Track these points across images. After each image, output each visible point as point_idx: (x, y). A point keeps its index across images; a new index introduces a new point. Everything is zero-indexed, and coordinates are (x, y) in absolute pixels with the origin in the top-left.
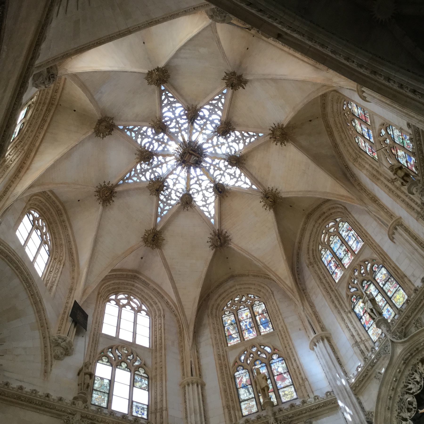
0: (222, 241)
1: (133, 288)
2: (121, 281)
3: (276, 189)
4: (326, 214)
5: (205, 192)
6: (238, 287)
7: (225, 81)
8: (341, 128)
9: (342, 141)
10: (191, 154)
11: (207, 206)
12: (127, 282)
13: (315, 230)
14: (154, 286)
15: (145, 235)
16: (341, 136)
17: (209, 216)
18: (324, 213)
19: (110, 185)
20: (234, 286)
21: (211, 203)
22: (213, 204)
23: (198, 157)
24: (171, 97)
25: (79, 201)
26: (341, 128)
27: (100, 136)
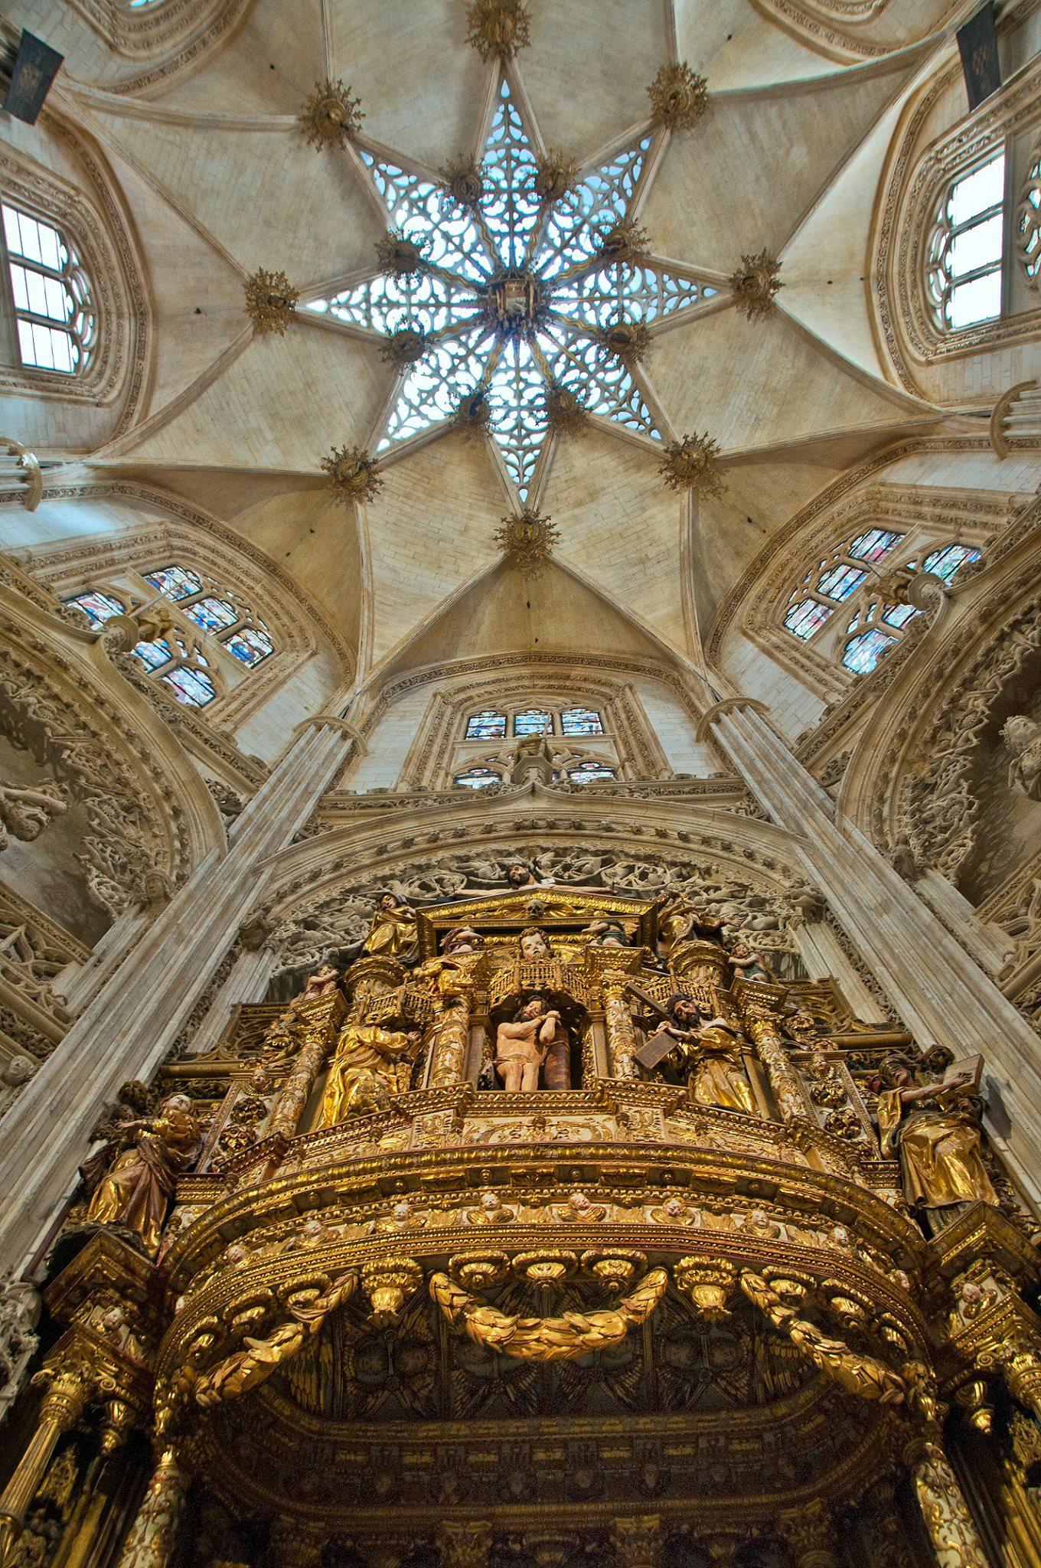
0: (357, 481)
1: (114, 318)
2: (118, 274)
3: (558, 534)
4: (568, 683)
5: (444, 388)
6: (258, 589)
7: (742, 266)
8: (785, 580)
9: (760, 598)
10: (527, 295)
11: (413, 412)
12: (122, 292)
13: (513, 684)
14: (146, 372)
15: (271, 277)
16: (766, 592)
17: (391, 430)
18: (568, 677)
19: (357, 122)
20: (254, 579)
21: (424, 417)
22: (426, 424)
23: (527, 312)
24: (632, 178)
25: (272, 67)
26: (785, 580)
27: (472, 27)
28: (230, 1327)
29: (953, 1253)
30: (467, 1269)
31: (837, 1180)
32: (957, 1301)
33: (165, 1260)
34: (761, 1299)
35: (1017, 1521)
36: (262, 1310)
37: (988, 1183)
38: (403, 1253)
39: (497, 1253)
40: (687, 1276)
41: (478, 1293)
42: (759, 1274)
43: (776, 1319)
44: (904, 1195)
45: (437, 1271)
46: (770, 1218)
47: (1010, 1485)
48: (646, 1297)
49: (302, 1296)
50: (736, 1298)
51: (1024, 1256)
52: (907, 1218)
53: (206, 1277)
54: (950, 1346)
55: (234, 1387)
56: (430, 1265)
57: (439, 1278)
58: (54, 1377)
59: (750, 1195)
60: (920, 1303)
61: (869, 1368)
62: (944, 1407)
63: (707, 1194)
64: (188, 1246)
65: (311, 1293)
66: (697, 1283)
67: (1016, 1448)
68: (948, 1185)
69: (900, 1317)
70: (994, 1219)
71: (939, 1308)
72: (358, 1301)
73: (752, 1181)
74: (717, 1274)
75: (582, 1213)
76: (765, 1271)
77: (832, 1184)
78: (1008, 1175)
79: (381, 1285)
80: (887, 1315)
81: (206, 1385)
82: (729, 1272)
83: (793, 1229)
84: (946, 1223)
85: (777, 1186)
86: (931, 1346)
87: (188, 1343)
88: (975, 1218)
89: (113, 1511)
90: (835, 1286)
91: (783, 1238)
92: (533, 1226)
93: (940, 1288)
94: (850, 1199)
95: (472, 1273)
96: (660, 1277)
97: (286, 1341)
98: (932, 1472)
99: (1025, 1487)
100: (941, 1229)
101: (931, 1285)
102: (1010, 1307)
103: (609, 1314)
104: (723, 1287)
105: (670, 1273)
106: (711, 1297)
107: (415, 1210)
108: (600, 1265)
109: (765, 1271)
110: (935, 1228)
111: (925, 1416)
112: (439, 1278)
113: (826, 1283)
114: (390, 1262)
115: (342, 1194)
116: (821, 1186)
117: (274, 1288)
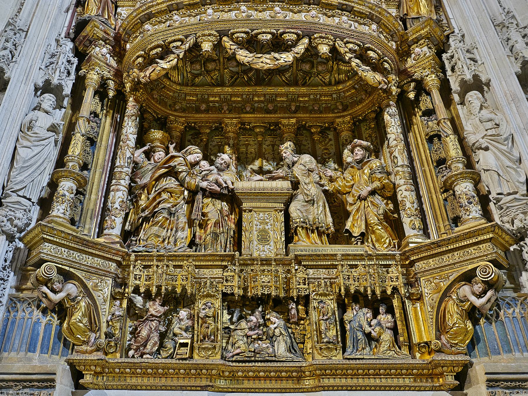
28: (149, 56)
29: (414, 36)
30: (236, 35)
31: (376, 6)
32: (411, 54)
33: (119, 30)
34: (342, 50)
35: (415, 126)
36: (160, 49)
37: (433, 9)
38: (212, 29)
39: (247, 30)
40: (316, 41)
41: (239, 45)
42: (342, 41)
43: (347, 58)
44: (399, 12)
45: (225, 36)
46: (349, 20)
47: (416, 116)
48: (301, 48)
49: (175, 44)
50: (334, 50)
51: (440, 39)
52: (399, 21)
53: (137, 37)
54: (405, 70)
55: (154, 76)
56: (222, 33)
57: (225, 39)
58: (88, 73)
59: (342, 10)
60: (397, 54)
61: (377, 76)
62: (399, 90)
63: (326, 9)
64: (128, 25)
65: (179, 43)
66: (320, 44)
67: (421, 105)
68: (417, 9)
69: (390, 59)
70: (433, 25)
71: (405, 56)
72: (197, 46)
73: (343, 5)
74: (327, 40)
75: (279, 15)
76: (345, 40)
77: (374, 7)
78: (441, 7)
79: (204, 41)
80: (386, 58)
81: (143, 75)
82: (332, 40)
83: (356, 24)
84: (413, 24)
85: (353, 7)
86: (399, 69)
87: (134, 61)
88: (426, 24)
89: (115, 115)
90: (369, 47)
91: (353, 28)
92: (261, 19)
93: (406, 49)
94: (380, 13)
95: (238, 37)
96: (306, 41)
97: (171, 60)
98: (391, 110)
99: (421, 117)
100: (411, 27)
101: (403, 48)
102: (431, 58)
103: (288, 54)
104: (329, 45)
105: (310, 39)
106: (325, 49)
107: (215, 12)
108: (285, 35)
109: (345, 40)
110: (408, 26)
111: (392, 93)
112: (225, 39)
113: (366, 45)
114: (207, 32)
115: (186, 5)
116: (370, 8)
117: (164, 41)
